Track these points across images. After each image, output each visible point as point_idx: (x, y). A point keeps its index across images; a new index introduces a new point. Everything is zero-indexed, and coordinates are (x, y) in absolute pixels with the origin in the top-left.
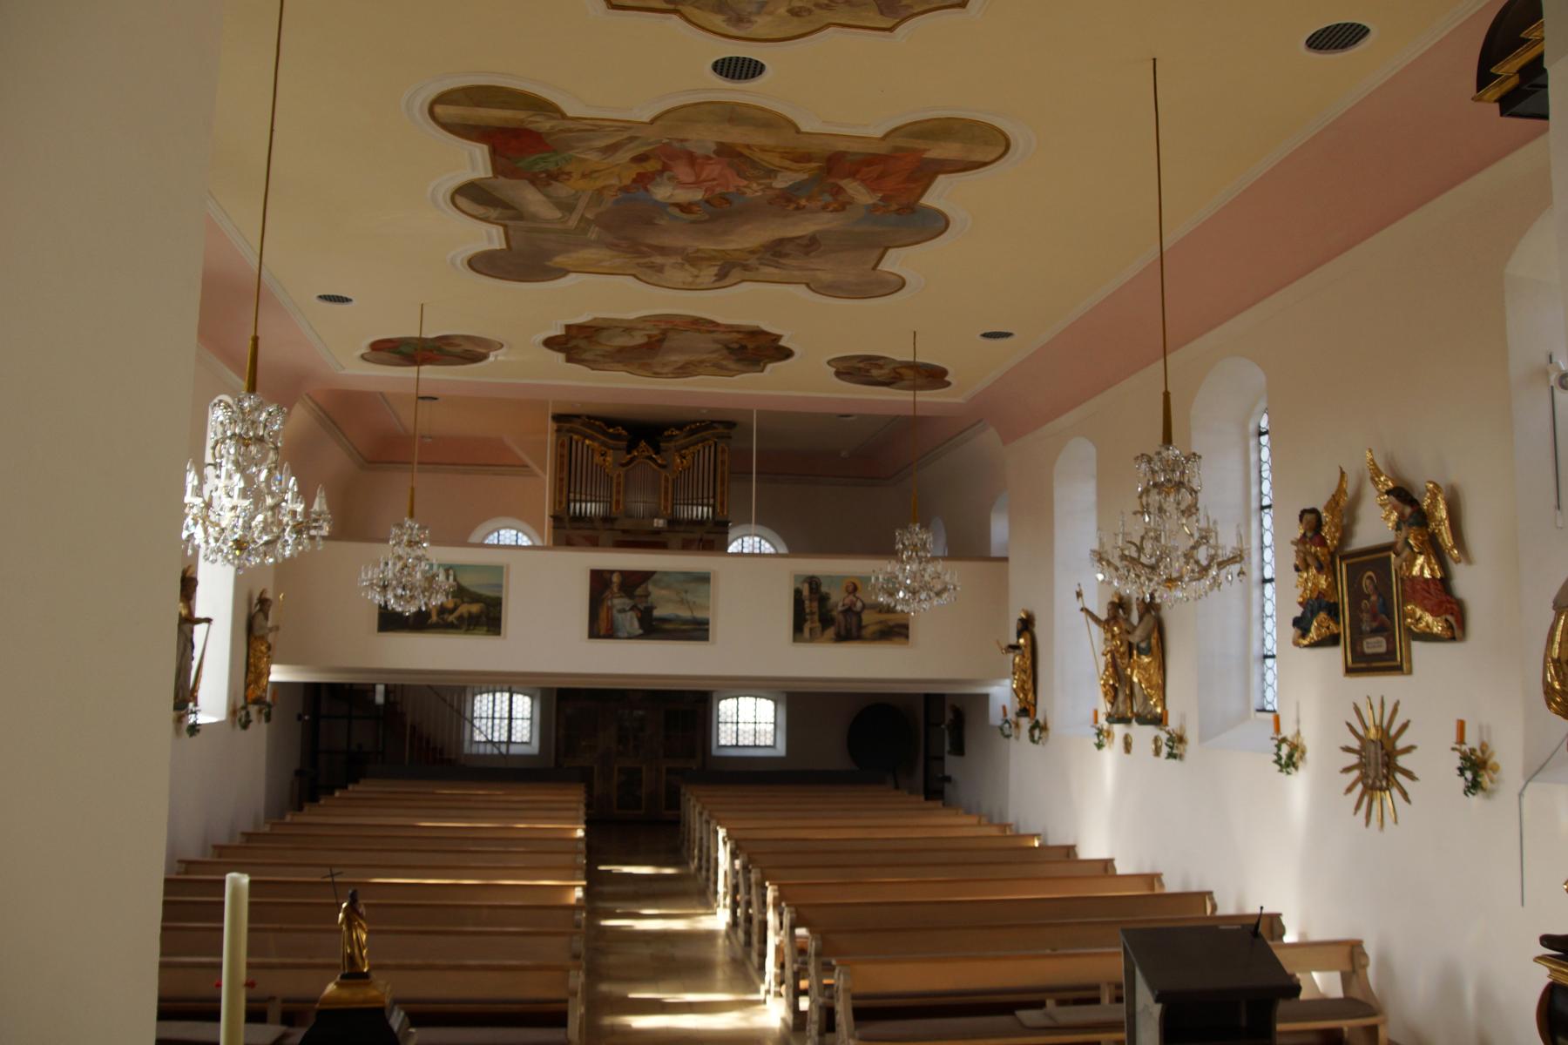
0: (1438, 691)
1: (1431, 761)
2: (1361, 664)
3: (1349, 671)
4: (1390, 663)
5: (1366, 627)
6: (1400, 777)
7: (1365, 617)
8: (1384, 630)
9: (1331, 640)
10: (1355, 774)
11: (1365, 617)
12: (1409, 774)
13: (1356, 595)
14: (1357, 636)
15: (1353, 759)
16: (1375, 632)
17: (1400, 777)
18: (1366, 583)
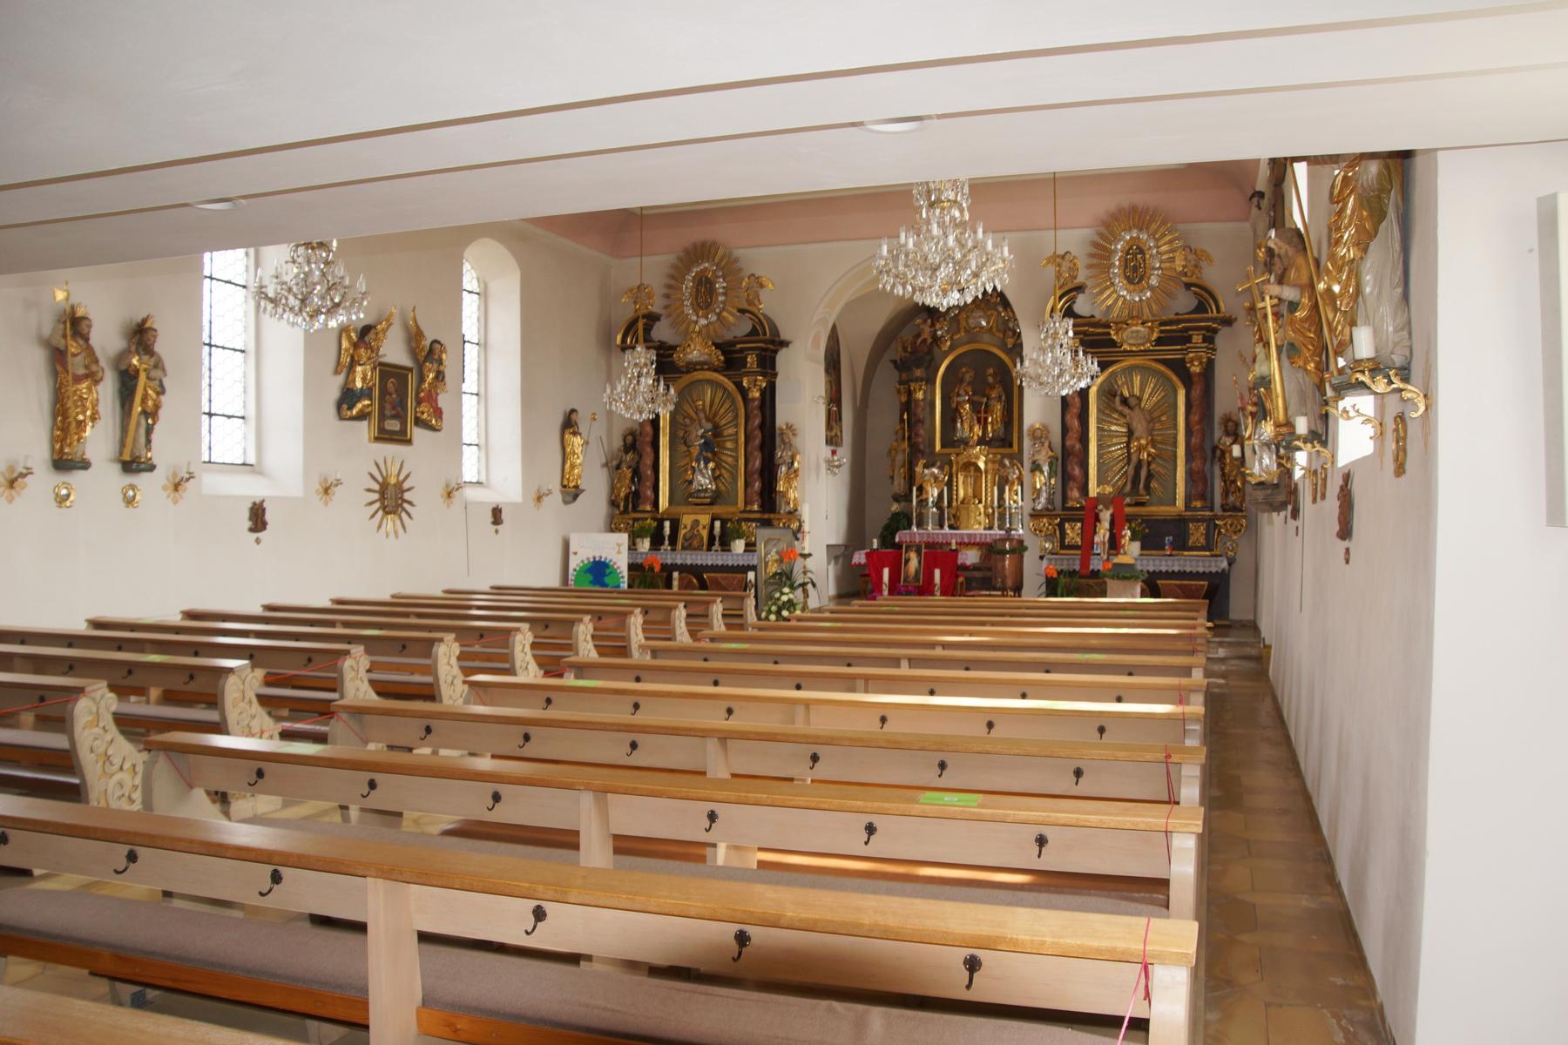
0: (417, 458)
1: (423, 495)
2: (384, 436)
3: (377, 439)
4: (402, 438)
5: (388, 413)
6: (406, 505)
7: (388, 406)
8: (401, 416)
9: (362, 416)
10: (377, 505)
11: (388, 406)
12: (410, 503)
13: (384, 392)
14: (382, 417)
15: (407, 496)
16: (393, 417)
17: (406, 505)
18: (390, 385)
